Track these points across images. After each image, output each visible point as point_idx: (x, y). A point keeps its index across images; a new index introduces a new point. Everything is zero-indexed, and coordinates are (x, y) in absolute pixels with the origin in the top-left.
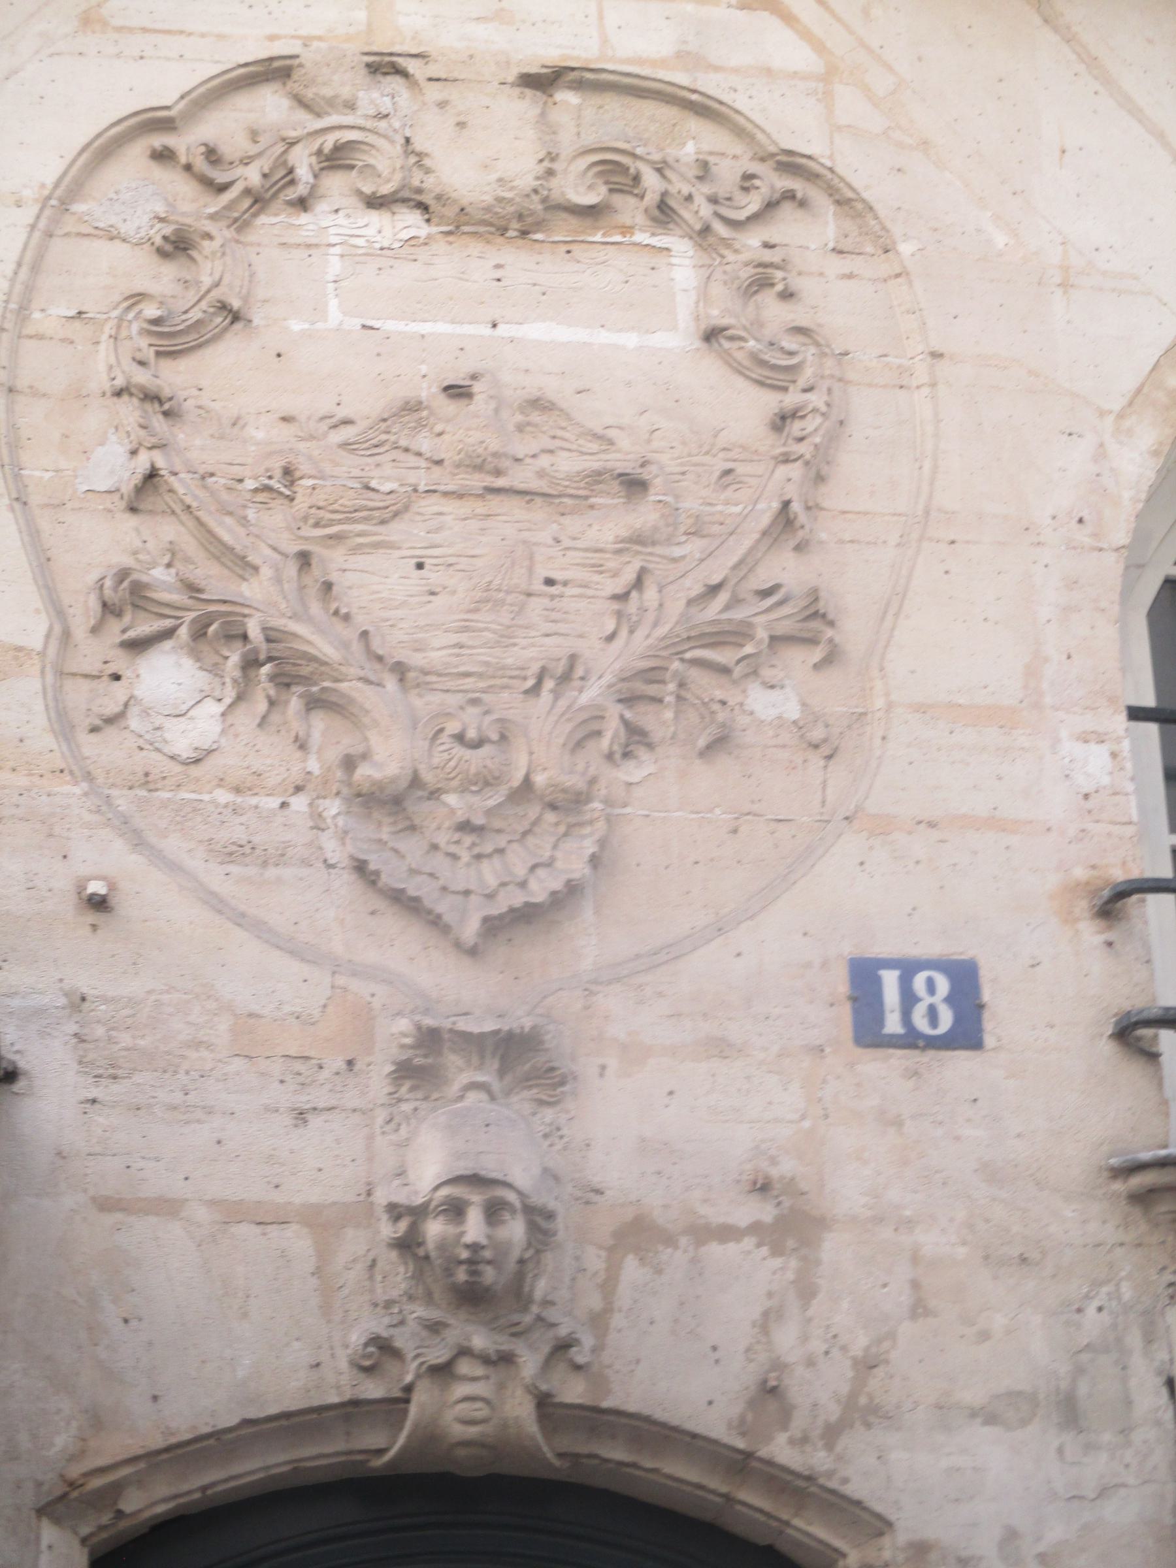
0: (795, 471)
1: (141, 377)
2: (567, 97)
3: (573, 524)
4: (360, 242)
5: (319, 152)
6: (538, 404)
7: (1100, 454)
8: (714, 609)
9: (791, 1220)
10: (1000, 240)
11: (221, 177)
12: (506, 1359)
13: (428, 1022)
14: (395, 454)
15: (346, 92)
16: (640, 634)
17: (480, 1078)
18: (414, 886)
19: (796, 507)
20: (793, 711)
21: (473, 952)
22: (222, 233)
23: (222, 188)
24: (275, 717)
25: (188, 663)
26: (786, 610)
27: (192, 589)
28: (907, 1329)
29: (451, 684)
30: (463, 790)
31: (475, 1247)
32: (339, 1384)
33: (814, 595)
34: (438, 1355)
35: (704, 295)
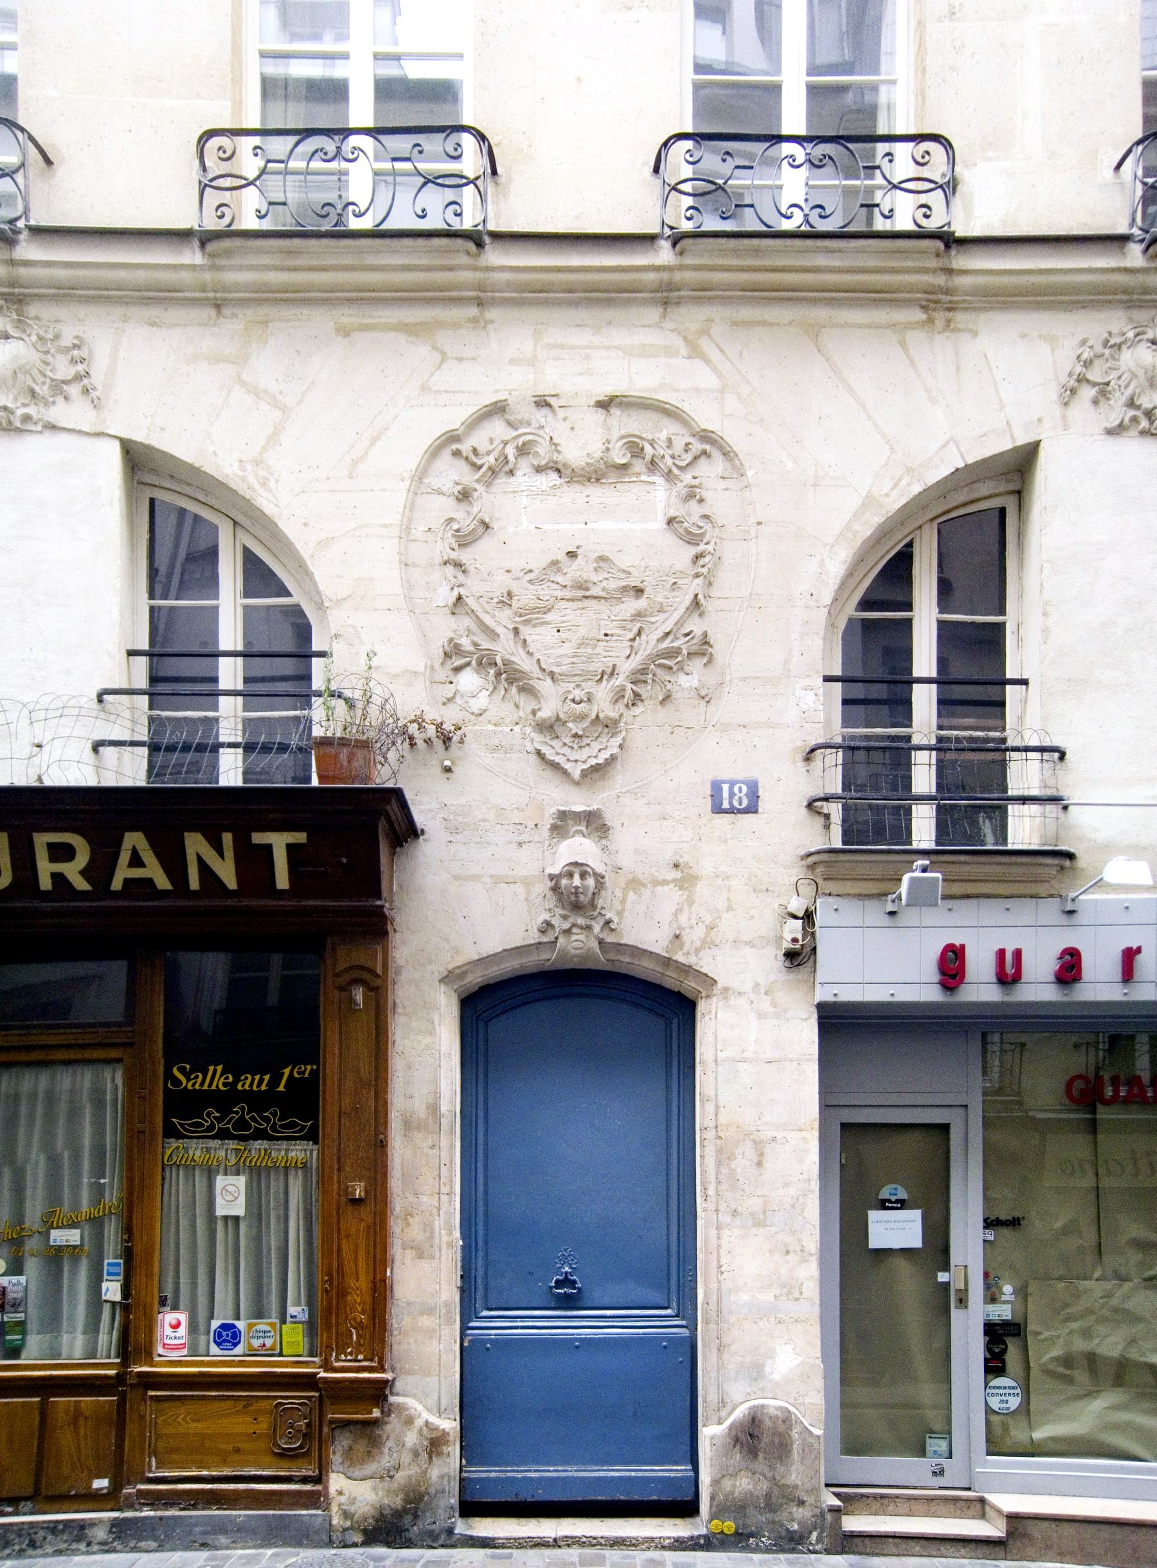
0: (700, 580)
1: (453, 555)
2: (616, 412)
3: (616, 609)
4: (534, 489)
5: (517, 447)
6: (602, 559)
7: (822, 563)
8: (666, 644)
9: (684, 875)
10: (790, 465)
11: (479, 462)
12: (589, 928)
13: (563, 808)
14: (549, 584)
15: (527, 417)
16: (639, 654)
17: (579, 828)
18: (557, 759)
19: (700, 597)
20: (695, 684)
21: (577, 783)
22: (480, 488)
23: (480, 467)
24: (508, 696)
25: (475, 675)
26: (694, 641)
27: (475, 644)
28: (725, 915)
29: (571, 679)
30: (574, 721)
31: (576, 888)
32: (534, 937)
33: (705, 635)
34: (566, 926)
35: (668, 505)
